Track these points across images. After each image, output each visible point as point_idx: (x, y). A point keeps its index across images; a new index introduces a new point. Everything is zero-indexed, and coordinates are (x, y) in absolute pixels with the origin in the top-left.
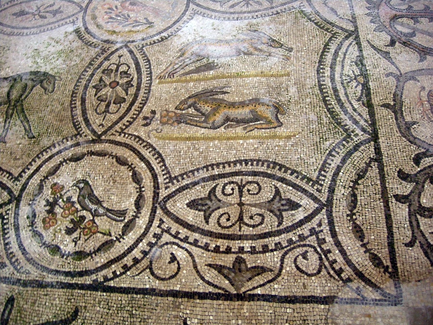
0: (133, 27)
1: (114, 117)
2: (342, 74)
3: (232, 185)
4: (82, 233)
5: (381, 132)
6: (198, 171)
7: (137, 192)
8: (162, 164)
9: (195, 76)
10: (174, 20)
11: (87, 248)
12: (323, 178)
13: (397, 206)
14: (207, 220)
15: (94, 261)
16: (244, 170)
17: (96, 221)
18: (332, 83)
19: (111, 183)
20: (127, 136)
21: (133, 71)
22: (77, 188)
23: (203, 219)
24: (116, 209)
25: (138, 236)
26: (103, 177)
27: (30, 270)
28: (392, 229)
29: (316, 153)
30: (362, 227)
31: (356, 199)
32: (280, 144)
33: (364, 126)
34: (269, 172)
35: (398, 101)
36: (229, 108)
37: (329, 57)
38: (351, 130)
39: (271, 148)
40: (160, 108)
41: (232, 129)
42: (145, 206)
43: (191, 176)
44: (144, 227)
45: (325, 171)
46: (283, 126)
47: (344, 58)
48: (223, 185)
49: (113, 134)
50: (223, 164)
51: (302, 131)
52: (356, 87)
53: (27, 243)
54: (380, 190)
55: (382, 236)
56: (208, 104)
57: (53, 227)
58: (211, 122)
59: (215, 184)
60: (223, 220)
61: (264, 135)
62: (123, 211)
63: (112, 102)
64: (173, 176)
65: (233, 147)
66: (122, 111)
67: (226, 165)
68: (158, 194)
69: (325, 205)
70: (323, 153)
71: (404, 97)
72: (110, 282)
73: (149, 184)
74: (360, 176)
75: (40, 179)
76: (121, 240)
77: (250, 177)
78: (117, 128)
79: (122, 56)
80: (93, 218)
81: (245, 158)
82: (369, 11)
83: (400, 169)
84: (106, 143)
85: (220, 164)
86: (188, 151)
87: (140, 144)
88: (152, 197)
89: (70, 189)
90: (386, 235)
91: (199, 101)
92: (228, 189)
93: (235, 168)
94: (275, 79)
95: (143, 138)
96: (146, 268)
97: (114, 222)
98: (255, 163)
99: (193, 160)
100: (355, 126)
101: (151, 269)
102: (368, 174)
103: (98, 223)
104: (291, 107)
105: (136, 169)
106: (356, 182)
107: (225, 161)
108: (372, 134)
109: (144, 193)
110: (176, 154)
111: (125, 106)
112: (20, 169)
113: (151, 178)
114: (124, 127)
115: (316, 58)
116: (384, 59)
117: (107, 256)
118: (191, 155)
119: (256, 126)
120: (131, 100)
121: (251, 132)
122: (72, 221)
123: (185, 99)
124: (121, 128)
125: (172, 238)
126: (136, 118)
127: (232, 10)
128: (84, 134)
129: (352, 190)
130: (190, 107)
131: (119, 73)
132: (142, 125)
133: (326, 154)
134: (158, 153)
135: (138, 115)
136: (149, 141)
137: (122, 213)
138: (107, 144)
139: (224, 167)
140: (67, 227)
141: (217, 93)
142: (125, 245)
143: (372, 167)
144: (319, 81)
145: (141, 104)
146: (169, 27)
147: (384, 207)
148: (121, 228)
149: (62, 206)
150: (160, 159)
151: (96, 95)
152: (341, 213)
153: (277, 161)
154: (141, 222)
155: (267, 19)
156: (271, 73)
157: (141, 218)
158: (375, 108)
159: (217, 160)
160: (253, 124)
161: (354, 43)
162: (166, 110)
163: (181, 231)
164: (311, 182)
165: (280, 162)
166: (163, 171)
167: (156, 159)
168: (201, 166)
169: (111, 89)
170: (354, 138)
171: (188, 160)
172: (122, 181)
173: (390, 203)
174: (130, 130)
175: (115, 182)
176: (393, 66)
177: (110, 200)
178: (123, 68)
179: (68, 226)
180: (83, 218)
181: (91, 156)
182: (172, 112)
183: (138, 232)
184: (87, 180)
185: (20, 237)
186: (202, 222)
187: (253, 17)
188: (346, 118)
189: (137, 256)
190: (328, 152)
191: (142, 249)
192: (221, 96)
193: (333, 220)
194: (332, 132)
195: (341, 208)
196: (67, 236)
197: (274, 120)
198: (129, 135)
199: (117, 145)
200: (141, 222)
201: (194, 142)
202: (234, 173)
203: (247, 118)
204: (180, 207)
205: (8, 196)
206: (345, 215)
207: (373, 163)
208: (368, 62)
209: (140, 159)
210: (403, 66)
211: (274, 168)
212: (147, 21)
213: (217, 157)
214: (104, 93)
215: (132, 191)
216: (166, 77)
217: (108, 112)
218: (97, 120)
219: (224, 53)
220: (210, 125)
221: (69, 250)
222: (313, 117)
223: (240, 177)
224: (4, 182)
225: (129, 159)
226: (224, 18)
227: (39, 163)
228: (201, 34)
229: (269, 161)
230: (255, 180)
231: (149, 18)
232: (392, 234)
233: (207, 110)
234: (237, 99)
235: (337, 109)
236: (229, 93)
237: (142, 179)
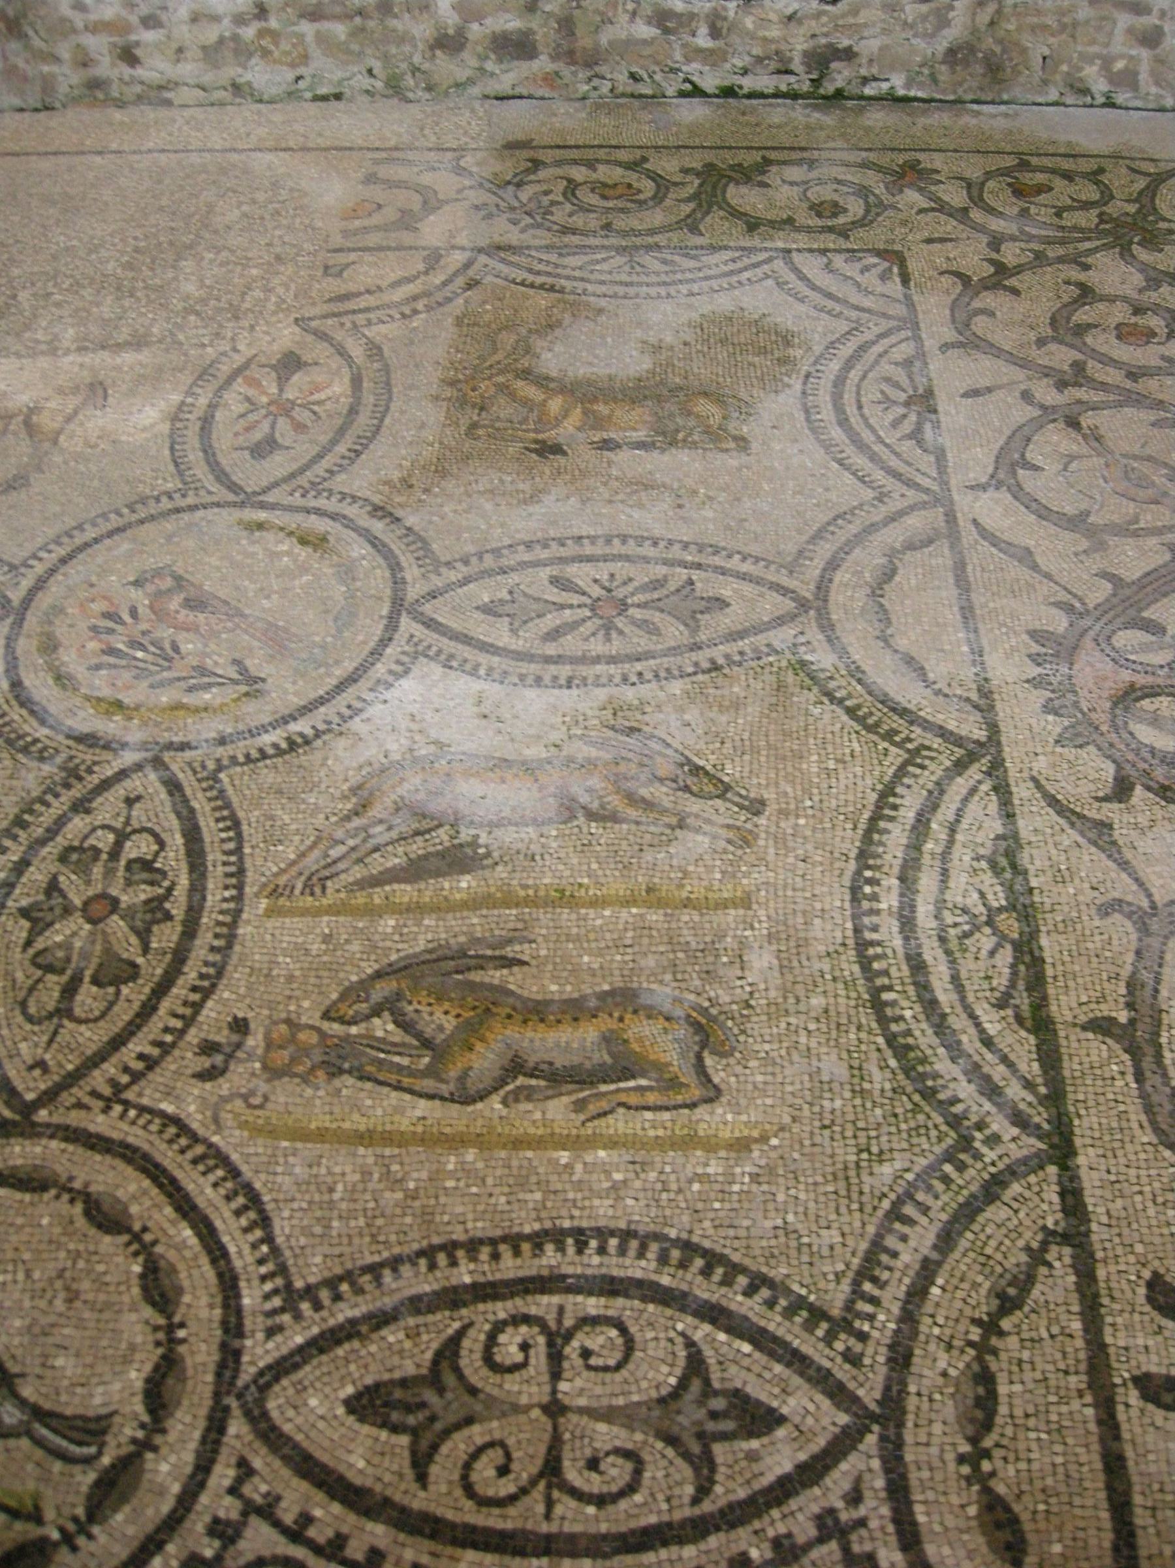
0: (190, 690)
1: (91, 1037)
2: (940, 905)
3: (524, 1329)
5: (1085, 1127)
6: (395, 1270)
7: (158, 1344)
8: (258, 1233)
9: (404, 892)
10: (339, 673)
12: (868, 1308)
13: (1147, 1420)
16: (570, 1270)
18: (906, 939)
20: (132, 1113)
21: (174, 858)
23: (407, 1463)
24: (68, 1412)
25: (150, 1528)
28: (1131, 1513)
29: (843, 1210)
30: (1016, 1508)
31: (992, 1394)
32: (710, 1170)
33: (1022, 1106)
34: (665, 1280)
35: (1145, 1010)
36: (525, 1022)
37: (896, 838)
38: (974, 1118)
39: (674, 1187)
40: (266, 1012)
41: (529, 1106)
42: (185, 1402)
44: (176, 1488)
45: (875, 1280)
46: (724, 1100)
47: (951, 842)
48: (487, 1327)
49: (79, 1105)
50: (493, 1242)
51: (794, 1119)
52: (992, 953)
54: (1082, 1355)
55: (1093, 1542)
56: (446, 1005)
58: (453, 1074)
59: (457, 1325)
60: (485, 1470)
61: (652, 1133)
62: (99, 1418)
63: (88, 974)
64: (299, 1284)
65: (534, 1179)
66: (123, 1014)
67: (503, 1248)
68: (237, 1354)
69: (874, 1418)
70: (868, 1209)
71: (1164, 993)
73: (204, 1313)
74: (1007, 1304)
76: (81, 1541)
77: (592, 1301)
78: (98, 1079)
79: (138, 798)
81: (576, 1223)
82: (1039, 670)
83: (1156, 1274)
84: (52, 1137)
85: (481, 1242)
86: (360, 1187)
87: (182, 1151)
88: (212, 1367)
90: (1108, 1538)
91: (415, 989)
92: (509, 1347)
93: (536, 1261)
94: (696, 918)
95: (195, 1126)
97: (57, 1466)
98: (613, 1242)
99: (380, 1222)
100: (988, 1106)
102: (1035, 1293)
104: (757, 1025)
105: (159, 1249)
106: (991, 1327)
107: (498, 1233)
108: (1048, 1135)
109: (182, 1349)
110: (317, 1198)
111: (134, 994)
113: (214, 1290)
115: (848, 841)
116: (1093, 849)
118: (371, 1205)
119: (623, 1098)
120: (159, 971)
121: (602, 1122)
123: (361, 982)
124: (113, 1082)
125: (282, 1540)
126: (174, 1045)
127: (551, 649)
129: (979, 1359)
130: (376, 1012)
131: (123, 863)
132: (194, 1076)
133: (880, 1213)
134: (248, 1189)
135: (182, 1032)
136: (215, 1139)
137: (92, 1426)
138: (54, 1144)
139: (496, 1256)
141: (481, 963)
143: (1050, 1265)
144: (857, 930)
145: (194, 989)
146: (322, 701)
147: (1100, 1422)
148: (84, 1489)
150: (252, 1215)
151: (28, 943)
152: (934, 1450)
153: (695, 1239)
154: (164, 1467)
155: (676, 687)
156: (684, 894)
157: (164, 1450)
158: (1062, 1034)
159: (470, 1225)
160: (612, 1087)
161: (985, 787)
162: (288, 1021)
163: (318, 1513)
164: (824, 1325)
165: (707, 1244)
166: (261, 1262)
167: (238, 1213)
168: (406, 1250)
169: (87, 927)
170: (984, 1150)
171: (362, 1222)
172: (102, 1297)
173: (1120, 1408)
174: (147, 1092)
176: (1124, 876)
177: (49, 1373)
178: (139, 847)
182: (312, 1027)
183: (150, 1512)
186: (401, 1476)
187: (625, 679)
188: (956, 1071)
190: (886, 1204)
192: (495, 976)
193: (904, 1477)
194: (903, 1126)
195: (937, 1428)
197: (688, 1077)
198: (143, 1109)
199: (92, 1148)
200: (164, 1467)
201: (387, 1152)
202: (531, 1279)
203: (588, 1065)
204: (320, 1411)
206: (950, 1457)
207: (1054, 1250)
208: (1033, 860)
209: (178, 1209)
210: (1160, 876)
211: (683, 1265)
212: (243, 670)
213: (470, 1216)
214: (59, 938)
215: (139, 1339)
216: (297, 892)
217: (69, 1014)
218: (23, 1046)
219: (513, 809)
220: (452, 1087)
222: (833, 1066)
223: (556, 1299)
225: (134, 1209)
226: (522, 677)
228: (433, 734)
229: (666, 1238)
230: (610, 1313)
231: (248, 663)
232: (1132, 1534)
233: (441, 1028)
234: (554, 988)
235: (924, 1037)
236: (523, 963)
237: (180, 1291)
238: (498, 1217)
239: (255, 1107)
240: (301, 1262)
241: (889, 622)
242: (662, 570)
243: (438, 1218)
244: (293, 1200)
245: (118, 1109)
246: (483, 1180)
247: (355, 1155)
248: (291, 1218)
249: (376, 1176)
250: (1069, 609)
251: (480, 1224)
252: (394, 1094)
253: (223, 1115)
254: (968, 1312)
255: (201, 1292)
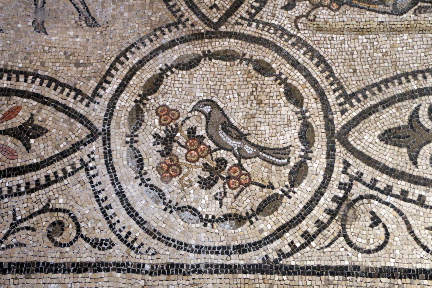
4: (227, 186)
8: (327, 73)
11: (241, 209)
14: (414, 161)
15: (257, 229)
17: (245, 165)
19: (254, 105)
22: (200, 113)
23: (408, 158)
24: (272, 147)
25: (316, 188)
26: (239, 95)
27: (156, 247)
41: (426, 15)
43: (377, 92)
44: (322, 173)
49: (237, 23)
50: (422, 72)
53: (141, 205)
57: (178, 178)
59: (415, 105)
62: (285, 149)
64: (349, 92)
68: (332, 120)
72: (288, 259)
73: (314, 105)
75: (134, 99)
76: (291, 194)
80: (240, 162)
87: (286, 41)
89: (189, 115)
95: (289, 29)
96: (339, 236)
97: (274, 167)
101: (346, 236)
103: (249, 170)
105: (289, 81)
107: (424, 68)
109: (309, 120)
110: (347, 57)
112: (92, 81)
113: (316, 96)
114: (253, 11)
117: (274, 219)
118: (370, 59)
122: (206, 167)
124: (248, 12)
125: (367, 189)
128: (190, 22)
132: (282, 8)
136: (299, 35)
138: (232, 40)
139: (425, 78)
140: (199, 177)
142: (298, 202)
148: (287, 175)
149: (184, 144)
154: (315, 165)
157: (313, 159)
159: (411, 66)
163: (378, 178)
171: (368, 66)
172: (272, 102)
174: (264, 16)
175: (260, 103)
179: (202, 176)
180: (222, 162)
181: (210, 59)
183: (315, 181)
184: (214, 99)
185: (124, 196)
186: (407, 163)
189: (321, 218)
191: (326, 206)
196: (203, 191)
201: (371, 37)
204: (370, 141)
205: (86, 129)
209: (292, 65)
215: (291, 118)
221: (212, 213)
224: (71, 105)
225: (274, 66)
227: (125, 73)
237: (302, 98)
238: (422, 62)
239: (311, 21)
240: (347, 83)
243: (398, 63)
244: (338, 59)
245: (254, 24)
246: (413, 46)
247: (358, 39)
248: (339, 66)
249: (369, 47)
251: (416, 65)
252: (368, 12)
253: (299, 24)
255: (311, 98)
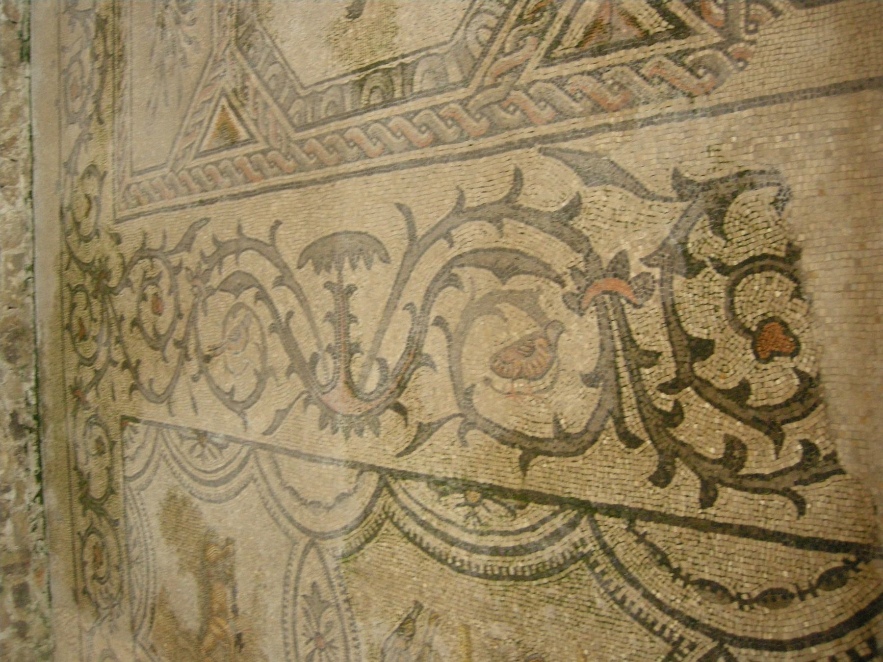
2: (464, 529)
5: (575, 491)
13: (722, 507)
18: (482, 552)
28: (768, 530)
29: (619, 629)
30: (765, 588)
31: (710, 583)
33: (566, 521)
35: (515, 439)
37: (429, 539)
38: (572, 549)
47: (431, 512)
51: (574, 639)
52: (489, 511)
54: (690, 531)
55: (782, 555)
69: (721, 645)
70: (618, 616)
71: (505, 425)
74: (664, 562)
82: (340, 430)
83: (650, 479)
90: (780, 546)
100: (565, 539)
102: (660, 545)
104: (530, 644)
106: (676, 573)
108: (580, 513)
115: (433, 566)
116: (432, 437)
129: (693, 583)
133: (621, 611)
143: (645, 533)
144: (479, 576)
147: (723, 533)
152: (737, 620)
155: (359, 624)
158: (528, 488)
161: (403, 485)
164: (676, 655)
173: (717, 520)
176: (446, 425)
188: (549, 549)
190: (616, 607)
193: (750, 639)
194: (577, 586)
195: (726, 616)
206: (740, 613)
207: (637, 529)
208: (440, 471)
210: (445, 406)
222: (548, 611)
232: (779, 533)
235: (532, 560)
241: (319, 502)
242: (299, 608)
250: (307, 402)
254: (669, 582)
